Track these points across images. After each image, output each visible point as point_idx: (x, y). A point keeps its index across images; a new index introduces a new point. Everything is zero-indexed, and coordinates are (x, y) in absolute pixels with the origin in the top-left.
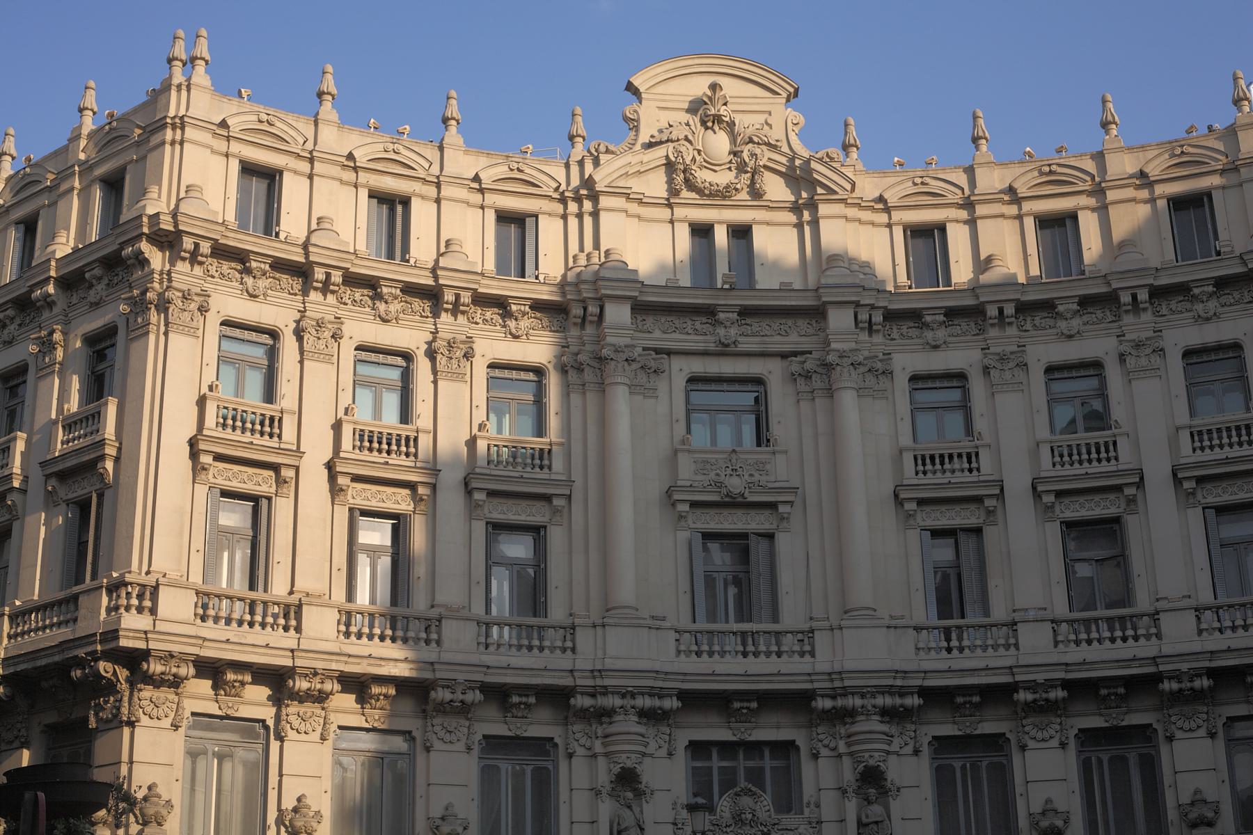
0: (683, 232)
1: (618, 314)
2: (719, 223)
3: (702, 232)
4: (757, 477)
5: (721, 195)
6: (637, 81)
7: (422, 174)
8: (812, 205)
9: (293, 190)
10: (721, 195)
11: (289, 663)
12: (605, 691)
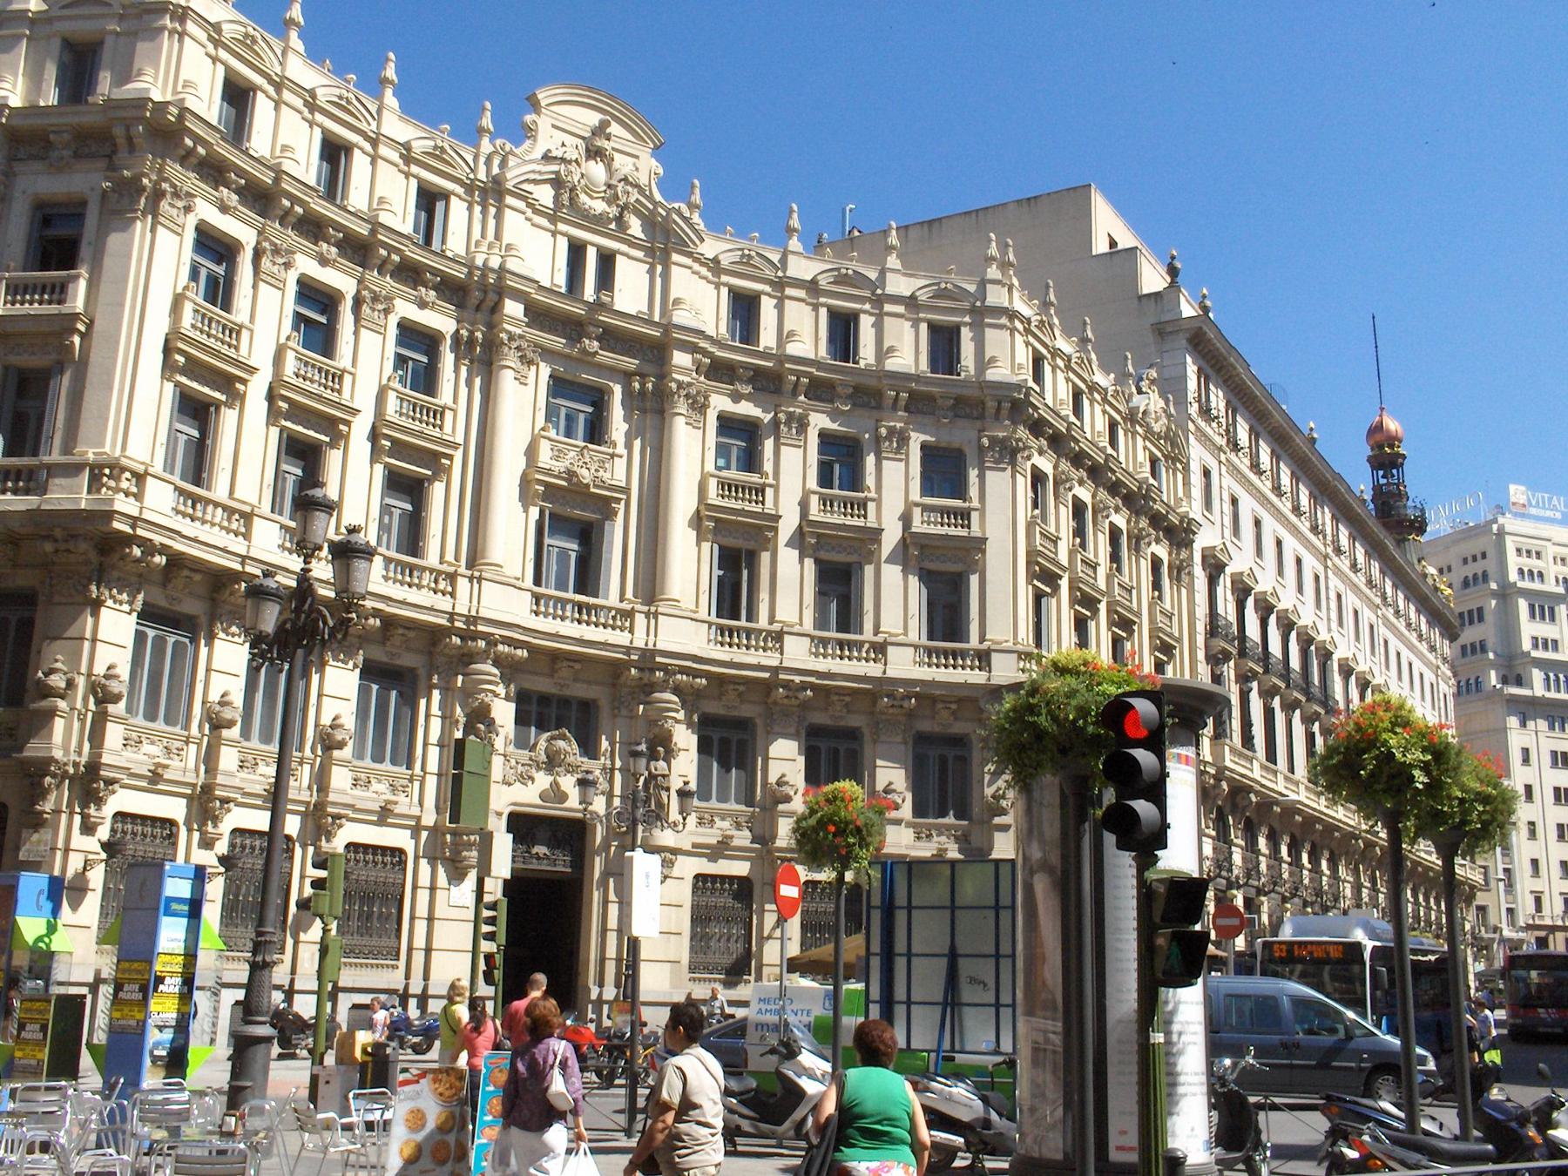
0: (563, 244)
1: (513, 309)
2: (593, 244)
3: (576, 252)
4: (601, 473)
5: (596, 222)
6: (544, 96)
7: (363, 126)
8: (666, 254)
9: (262, 108)
10: (596, 222)
11: (238, 567)
12: (475, 636)
